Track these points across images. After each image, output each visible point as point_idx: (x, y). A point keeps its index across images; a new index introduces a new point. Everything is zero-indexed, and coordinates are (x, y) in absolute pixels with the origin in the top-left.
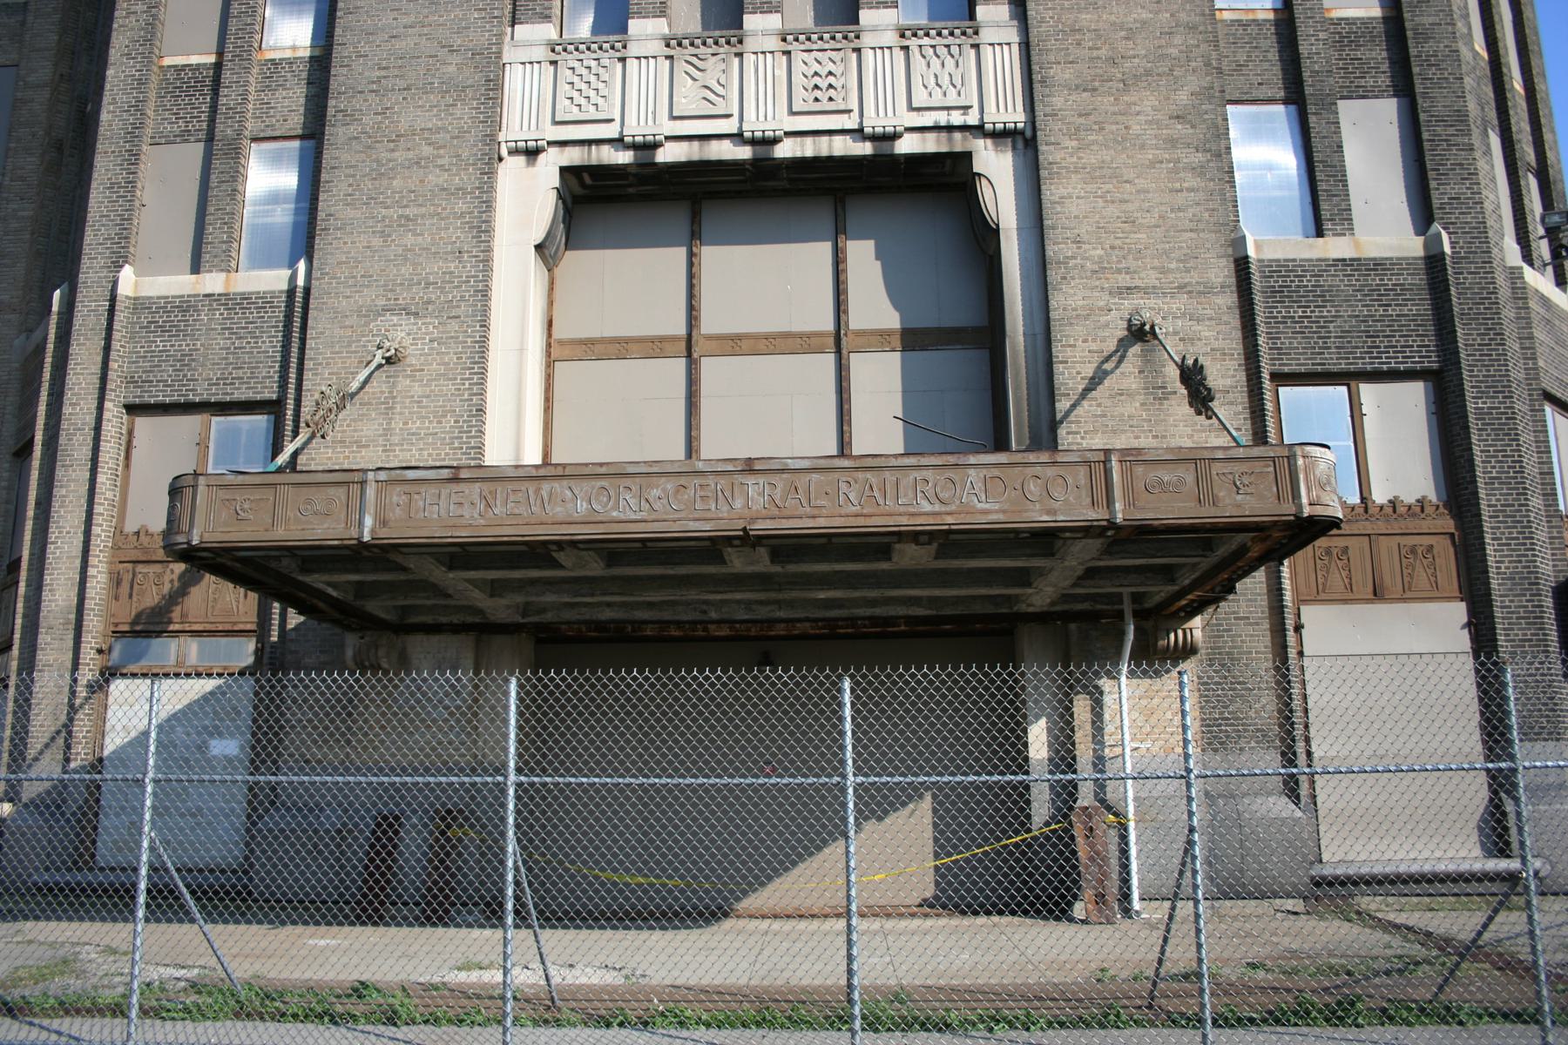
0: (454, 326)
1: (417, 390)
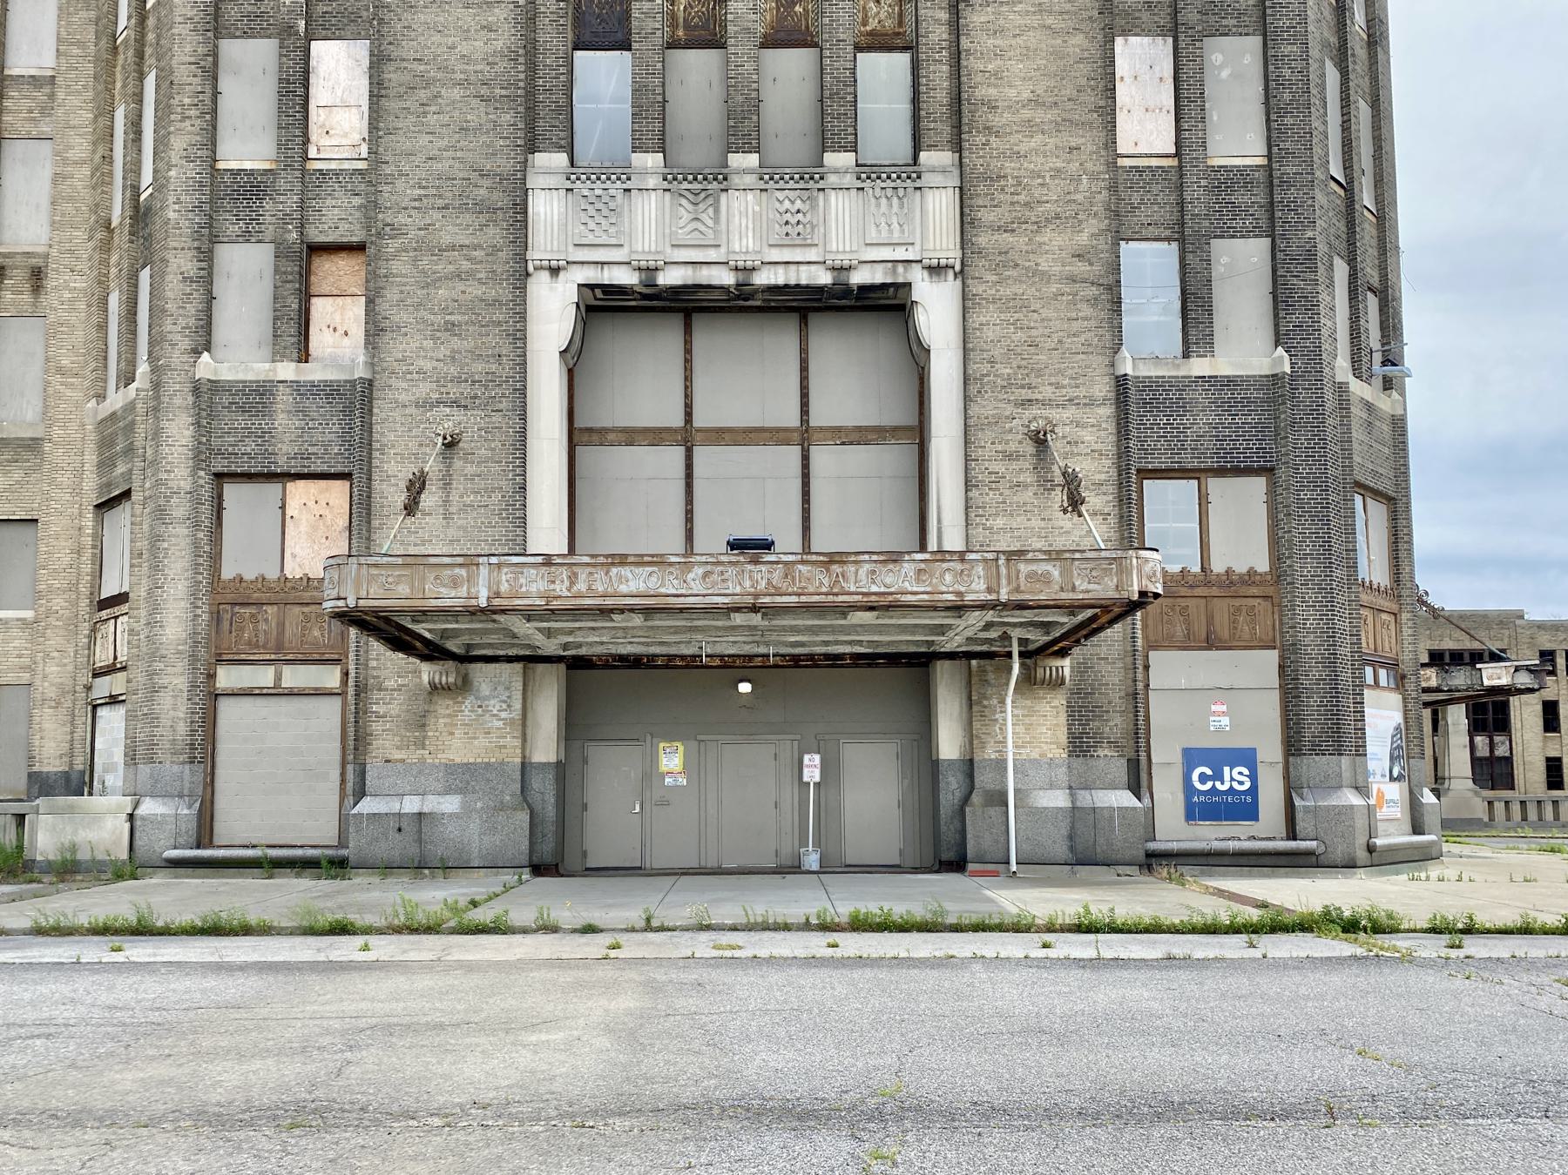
0: (497, 418)
1: (470, 469)
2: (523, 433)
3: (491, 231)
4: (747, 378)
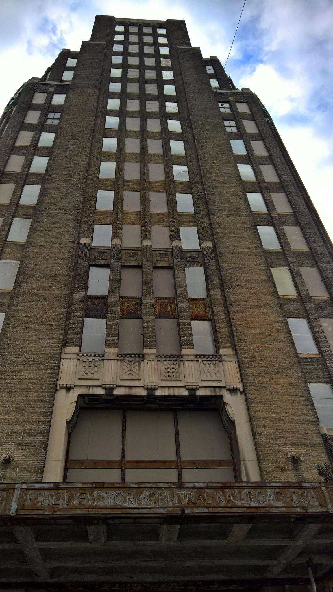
0: (33, 450)
2: (44, 461)
3: (43, 373)
4: (151, 439)
